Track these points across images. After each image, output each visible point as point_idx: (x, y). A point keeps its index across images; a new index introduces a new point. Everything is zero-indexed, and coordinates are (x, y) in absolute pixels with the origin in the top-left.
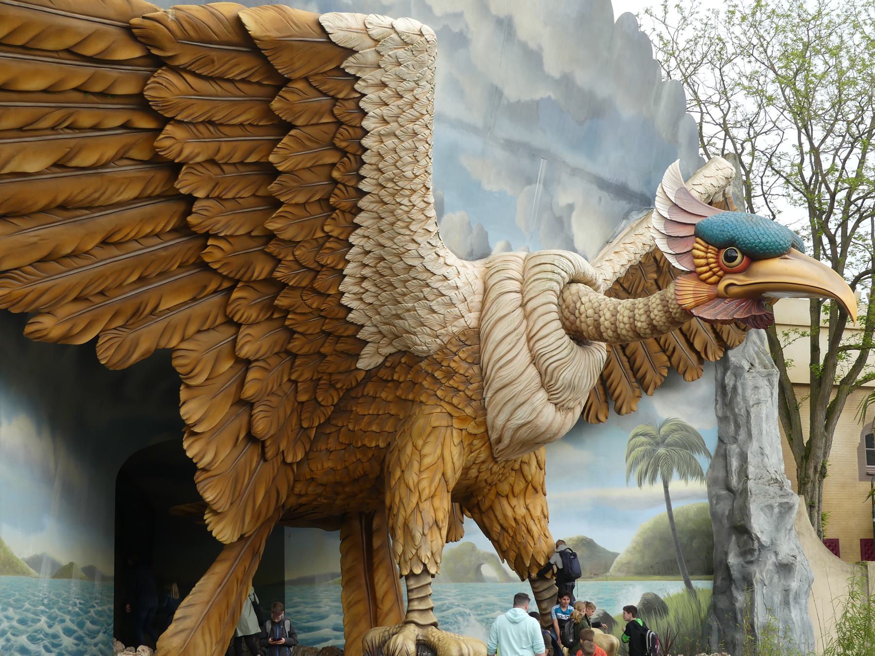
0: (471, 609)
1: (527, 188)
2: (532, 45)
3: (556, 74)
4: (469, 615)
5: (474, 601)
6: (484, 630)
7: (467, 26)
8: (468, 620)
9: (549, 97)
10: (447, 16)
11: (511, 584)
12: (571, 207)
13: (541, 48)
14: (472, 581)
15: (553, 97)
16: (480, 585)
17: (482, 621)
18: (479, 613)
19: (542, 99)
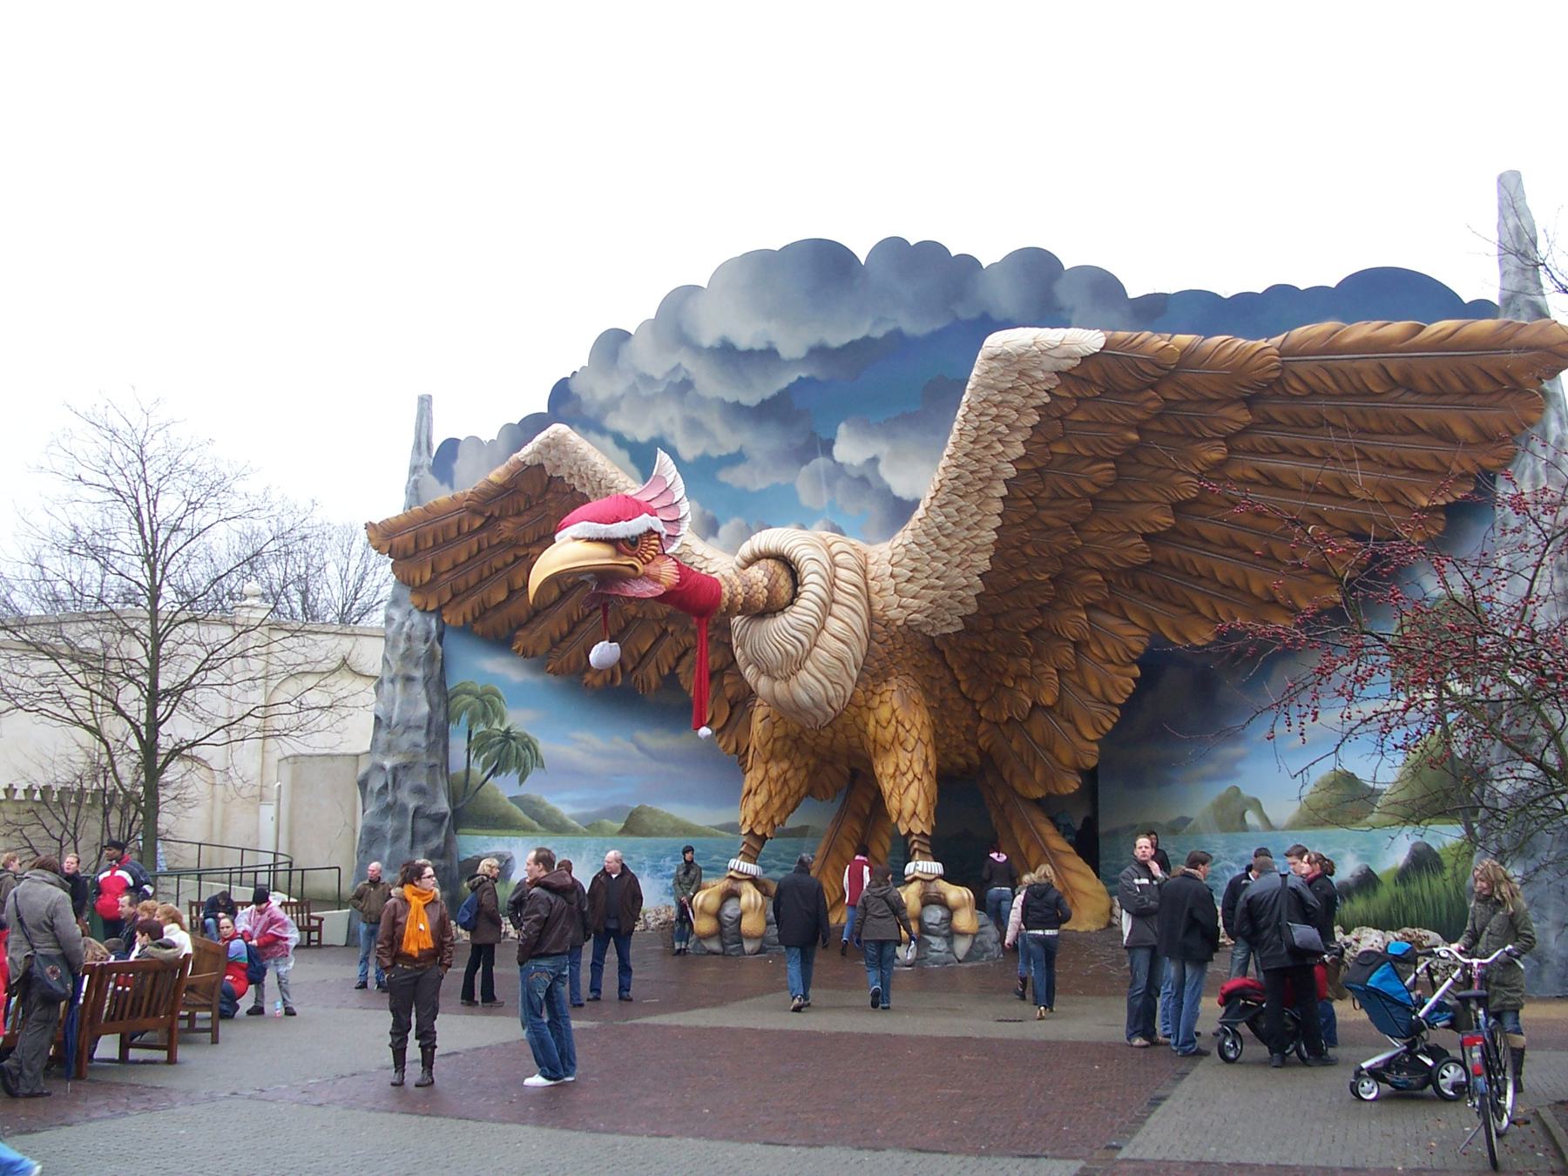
0: (1236, 862)
1: (804, 469)
2: (759, 345)
3: (800, 352)
7: (686, 371)
9: (800, 378)
10: (667, 374)
11: (1271, 833)
13: (769, 343)
14: (1237, 831)
15: (804, 375)
19: (791, 386)
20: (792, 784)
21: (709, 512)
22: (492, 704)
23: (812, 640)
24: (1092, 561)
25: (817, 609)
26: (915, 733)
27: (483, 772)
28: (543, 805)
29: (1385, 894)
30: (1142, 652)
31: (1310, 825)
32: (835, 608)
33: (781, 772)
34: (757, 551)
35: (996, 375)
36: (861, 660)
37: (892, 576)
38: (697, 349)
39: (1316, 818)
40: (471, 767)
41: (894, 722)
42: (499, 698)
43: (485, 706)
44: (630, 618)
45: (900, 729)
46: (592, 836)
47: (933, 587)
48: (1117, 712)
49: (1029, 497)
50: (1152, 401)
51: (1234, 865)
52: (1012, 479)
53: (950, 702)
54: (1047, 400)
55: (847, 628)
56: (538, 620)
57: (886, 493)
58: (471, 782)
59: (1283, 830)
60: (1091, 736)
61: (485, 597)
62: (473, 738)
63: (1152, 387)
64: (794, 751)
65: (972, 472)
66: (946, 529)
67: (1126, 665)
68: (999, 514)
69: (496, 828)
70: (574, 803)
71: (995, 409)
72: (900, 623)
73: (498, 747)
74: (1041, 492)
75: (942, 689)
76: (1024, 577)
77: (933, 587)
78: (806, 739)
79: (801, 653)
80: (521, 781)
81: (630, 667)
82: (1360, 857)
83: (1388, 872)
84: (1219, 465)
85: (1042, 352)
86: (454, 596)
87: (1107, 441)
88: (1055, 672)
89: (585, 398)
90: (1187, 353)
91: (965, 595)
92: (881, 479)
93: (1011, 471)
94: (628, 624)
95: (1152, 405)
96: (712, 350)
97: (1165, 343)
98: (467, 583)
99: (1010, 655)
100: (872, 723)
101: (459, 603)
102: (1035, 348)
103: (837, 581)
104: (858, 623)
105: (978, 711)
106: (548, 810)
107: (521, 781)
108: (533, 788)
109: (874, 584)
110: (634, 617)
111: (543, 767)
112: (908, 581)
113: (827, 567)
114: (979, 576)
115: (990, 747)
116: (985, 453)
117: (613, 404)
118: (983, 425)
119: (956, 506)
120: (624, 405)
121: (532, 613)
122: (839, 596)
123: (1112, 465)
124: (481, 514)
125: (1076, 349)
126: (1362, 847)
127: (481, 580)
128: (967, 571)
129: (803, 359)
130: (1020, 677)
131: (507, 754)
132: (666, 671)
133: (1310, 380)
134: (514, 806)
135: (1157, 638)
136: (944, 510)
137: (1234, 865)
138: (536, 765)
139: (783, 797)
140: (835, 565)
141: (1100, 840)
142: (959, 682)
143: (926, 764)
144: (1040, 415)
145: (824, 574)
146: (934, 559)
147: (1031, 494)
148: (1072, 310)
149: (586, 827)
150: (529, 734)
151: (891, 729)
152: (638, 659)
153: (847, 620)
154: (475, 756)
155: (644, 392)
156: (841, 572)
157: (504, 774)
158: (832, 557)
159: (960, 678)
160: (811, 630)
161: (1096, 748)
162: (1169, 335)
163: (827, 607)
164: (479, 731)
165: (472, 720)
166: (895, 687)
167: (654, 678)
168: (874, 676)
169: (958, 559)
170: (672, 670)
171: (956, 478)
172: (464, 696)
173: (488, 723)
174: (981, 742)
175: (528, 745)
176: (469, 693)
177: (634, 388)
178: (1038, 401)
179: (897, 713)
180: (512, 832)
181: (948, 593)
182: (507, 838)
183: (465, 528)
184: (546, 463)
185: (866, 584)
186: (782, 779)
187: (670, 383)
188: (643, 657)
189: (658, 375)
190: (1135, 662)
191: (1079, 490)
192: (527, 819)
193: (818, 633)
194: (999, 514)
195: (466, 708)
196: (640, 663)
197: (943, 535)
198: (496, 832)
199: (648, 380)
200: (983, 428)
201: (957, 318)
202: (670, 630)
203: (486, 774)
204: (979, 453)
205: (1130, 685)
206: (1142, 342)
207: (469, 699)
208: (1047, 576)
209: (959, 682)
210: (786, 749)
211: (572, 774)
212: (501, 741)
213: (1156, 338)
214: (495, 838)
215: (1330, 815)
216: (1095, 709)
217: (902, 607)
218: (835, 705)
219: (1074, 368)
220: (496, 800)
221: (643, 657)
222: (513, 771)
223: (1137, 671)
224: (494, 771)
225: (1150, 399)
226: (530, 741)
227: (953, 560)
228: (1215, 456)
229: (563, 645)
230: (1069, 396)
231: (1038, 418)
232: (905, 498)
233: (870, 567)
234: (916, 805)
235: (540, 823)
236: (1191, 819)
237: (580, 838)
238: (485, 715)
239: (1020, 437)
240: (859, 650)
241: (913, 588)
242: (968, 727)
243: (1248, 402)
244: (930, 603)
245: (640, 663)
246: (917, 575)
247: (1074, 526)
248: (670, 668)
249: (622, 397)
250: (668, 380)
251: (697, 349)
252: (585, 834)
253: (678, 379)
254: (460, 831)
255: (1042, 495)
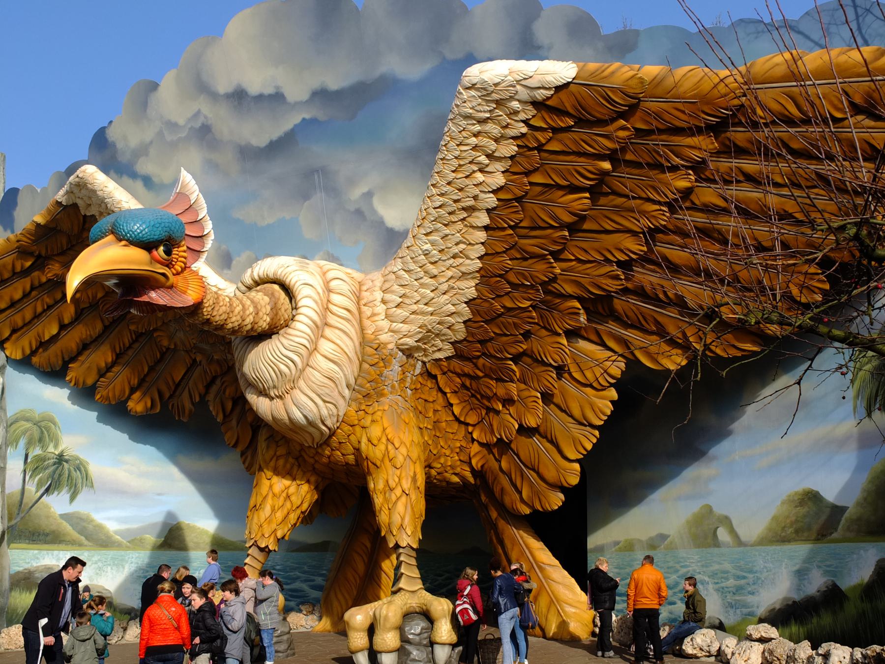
0: (709, 577)
1: (307, 203)
3: (305, 96)
4: (708, 583)
5: (711, 569)
6: (720, 600)
7: (206, 117)
8: (707, 589)
9: (304, 119)
10: (190, 120)
11: (741, 549)
12: (369, 195)
13: (277, 87)
14: (710, 547)
16: (716, 550)
17: (717, 590)
18: (716, 581)
19: (295, 126)
20: (293, 498)
21: (224, 247)
22: (48, 429)
23: (305, 361)
24: (570, 289)
25: (308, 331)
26: (403, 450)
27: (37, 492)
28: (92, 521)
29: (851, 609)
30: (619, 376)
31: (778, 541)
32: (328, 332)
33: (284, 489)
34: (256, 278)
35: (474, 104)
36: (352, 381)
37: (384, 302)
38: (213, 96)
39: (783, 534)
40: (27, 487)
41: (384, 440)
42: (55, 424)
43: (42, 432)
44: (164, 350)
45: (390, 447)
46: (134, 549)
47: (423, 313)
48: (597, 433)
49: (511, 227)
50: (621, 130)
51: (707, 579)
52: (494, 209)
53: (444, 424)
54: (524, 130)
55: (339, 350)
56: (87, 353)
57: (380, 223)
58: (25, 501)
59: (752, 546)
60: (573, 455)
61: (41, 332)
62: (29, 460)
63: (622, 115)
64: (295, 468)
65: (456, 201)
66: (433, 256)
67: (604, 388)
68: (482, 243)
69: (46, 543)
70: (119, 520)
71: (474, 139)
72: (391, 346)
73: (52, 469)
74: (521, 221)
75: (435, 411)
76: (509, 304)
77: (423, 313)
78: (306, 457)
79: (294, 371)
80: (72, 499)
81: (167, 395)
82: (826, 573)
83: (855, 588)
84: (687, 193)
85: (518, 82)
86: (14, 331)
87: (578, 168)
88: (539, 395)
89: (120, 145)
90: (657, 82)
91: (453, 321)
92: (374, 211)
93: (491, 201)
94: (163, 355)
95: (622, 134)
96: (229, 96)
97: (631, 73)
98: (24, 319)
99: (499, 380)
100: (364, 440)
101: (18, 339)
102: (509, 78)
103: (331, 307)
104: (350, 346)
105: (471, 433)
106: (95, 526)
107: (72, 499)
108: (84, 505)
109: (367, 311)
110: (168, 349)
111: (92, 486)
112: (398, 306)
113: (320, 291)
114: (466, 303)
115: (482, 466)
116: (467, 181)
117: (142, 151)
118: (464, 154)
119: (442, 234)
120: (152, 151)
121: (81, 347)
122: (332, 319)
123: (587, 195)
124: (31, 254)
125: (549, 78)
126: (828, 563)
127: (37, 317)
128: (453, 298)
129: (307, 101)
130: (508, 401)
131: (60, 475)
132: (197, 399)
133: (775, 106)
134: (65, 523)
135: (632, 363)
136: (429, 238)
137: (707, 579)
138: (86, 485)
139: (285, 512)
140: (330, 291)
141: (589, 555)
142: (451, 405)
143: (414, 480)
144: (518, 146)
145: (317, 298)
146: (422, 285)
147: (512, 224)
148: (550, 48)
149: (129, 542)
150: (81, 457)
151: (382, 447)
152: (173, 388)
153: (338, 342)
154: (31, 477)
155: (169, 138)
156: (335, 298)
157: (56, 493)
158: (327, 283)
159: (452, 402)
160: (304, 352)
161: (577, 466)
162: (638, 66)
163: (320, 328)
164: (35, 454)
165: (30, 444)
166: (386, 408)
167: (188, 405)
168: (367, 396)
169: (445, 287)
170: (202, 397)
171: (440, 207)
172: (23, 423)
173: (44, 447)
174: (474, 462)
175: (80, 467)
176: (27, 420)
177: (160, 134)
178: (515, 131)
179: (387, 431)
180: (62, 546)
181: (436, 318)
182: (56, 552)
183: (18, 269)
184: (80, 203)
185: (359, 309)
186: (284, 495)
187: (191, 128)
188: (177, 386)
189: (181, 122)
190: (611, 385)
191: (555, 218)
192: (75, 535)
193: (310, 354)
194: (482, 243)
195: (24, 433)
196: (175, 392)
197: (432, 263)
198: (46, 546)
199: (172, 126)
200: (464, 158)
201: (444, 58)
202: (198, 359)
203: (39, 494)
204: (461, 183)
205: (608, 407)
206: (613, 73)
207: (28, 425)
208: (528, 303)
209: (451, 405)
210: (288, 466)
211: (119, 492)
212: (55, 464)
213: (626, 68)
214: (45, 552)
215: (797, 531)
216: (576, 431)
217: (393, 331)
218: (329, 423)
219: (548, 98)
220: (48, 517)
221: (177, 386)
222: (65, 489)
223: (613, 394)
224: (47, 490)
225: (623, 128)
226: (81, 463)
227: (441, 287)
228: (683, 184)
229: (109, 375)
230: (544, 126)
231: (516, 148)
232: (397, 229)
233: (364, 294)
234: (403, 519)
235: (87, 538)
236: (669, 536)
237: (123, 553)
238: (41, 440)
239: (499, 166)
240: (350, 371)
241: (402, 313)
242: (461, 447)
243: (717, 129)
244: (419, 327)
245: (175, 392)
246: (407, 301)
247: (552, 253)
248: (200, 395)
249: (151, 143)
250: (189, 126)
251: (213, 96)
252: (128, 548)
253: (198, 125)
254: (12, 545)
255: (522, 225)
